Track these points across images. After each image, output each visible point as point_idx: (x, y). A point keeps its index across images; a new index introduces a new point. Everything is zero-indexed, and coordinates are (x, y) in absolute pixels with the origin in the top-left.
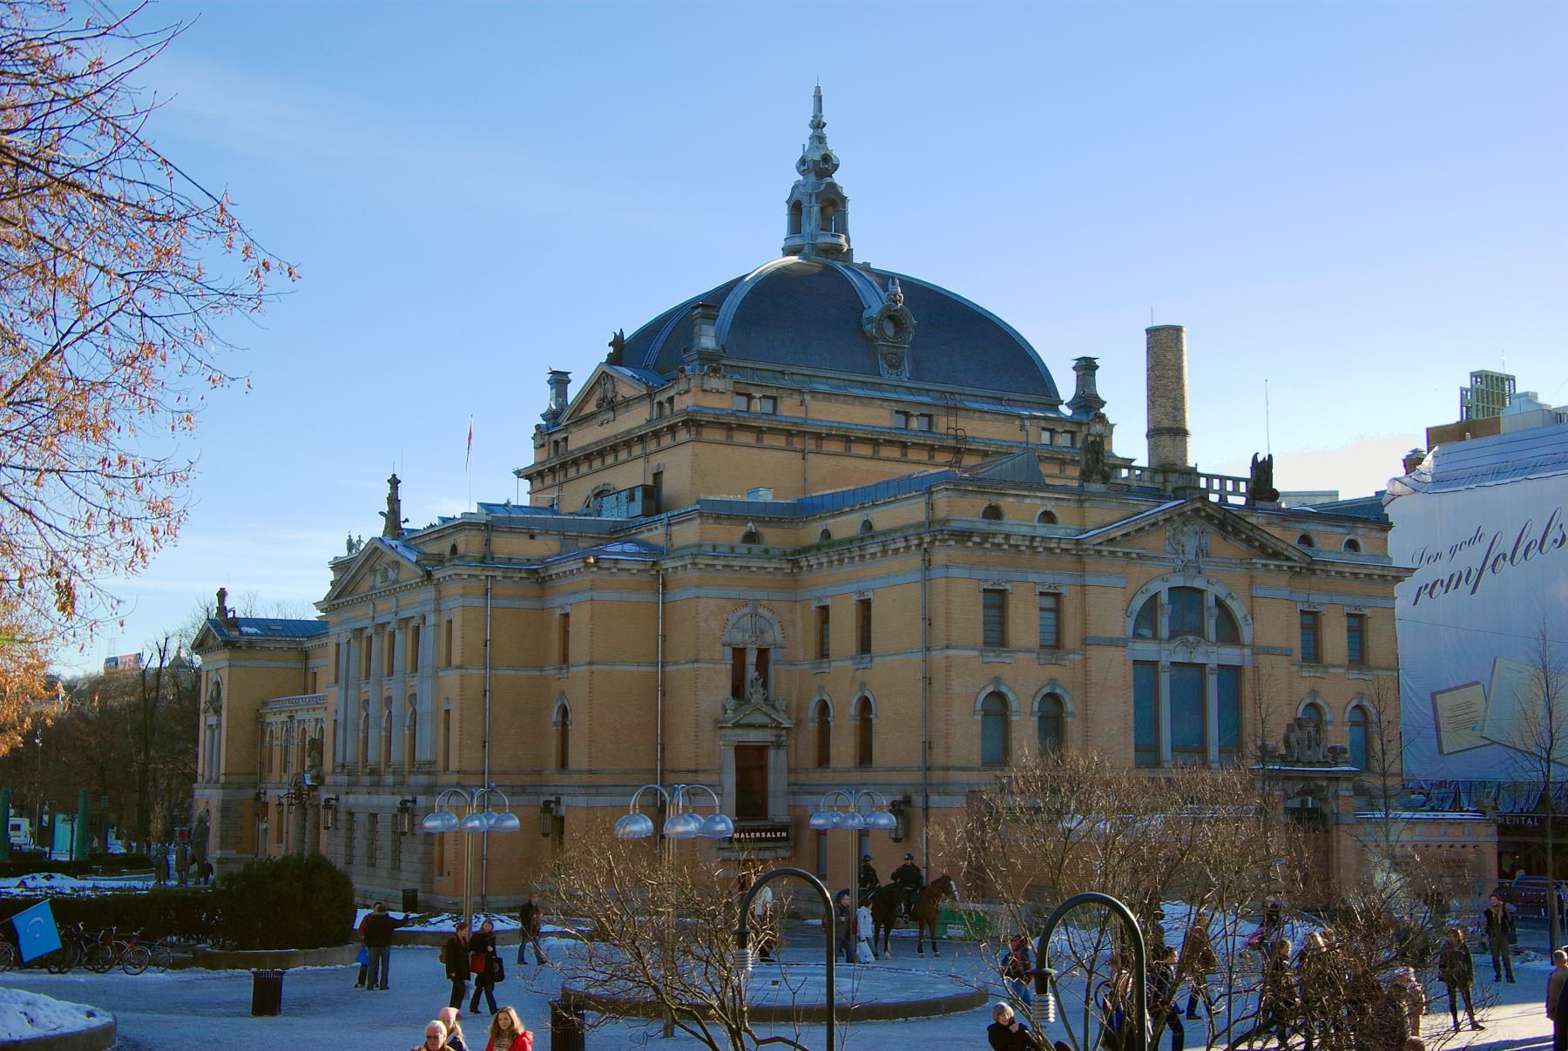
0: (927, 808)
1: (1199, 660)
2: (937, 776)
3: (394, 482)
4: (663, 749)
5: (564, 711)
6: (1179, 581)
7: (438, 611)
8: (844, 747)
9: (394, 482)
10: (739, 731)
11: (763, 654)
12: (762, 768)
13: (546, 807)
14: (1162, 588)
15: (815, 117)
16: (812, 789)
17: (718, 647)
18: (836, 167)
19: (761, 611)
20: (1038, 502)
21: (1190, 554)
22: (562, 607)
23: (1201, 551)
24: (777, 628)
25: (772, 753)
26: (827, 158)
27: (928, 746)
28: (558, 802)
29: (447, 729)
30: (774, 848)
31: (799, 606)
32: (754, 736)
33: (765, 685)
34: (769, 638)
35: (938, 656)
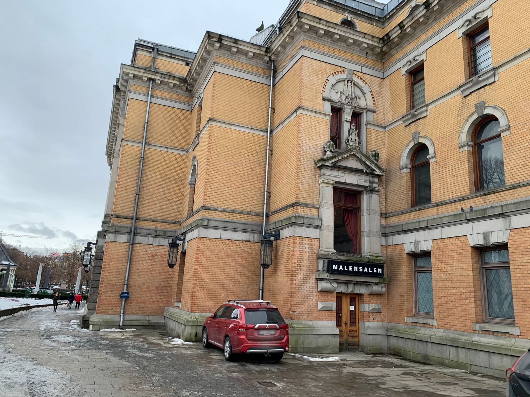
4: (269, 196)
8: (450, 177)
10: (336, 173)
11: (356, 116)
19: (355, 79)
30: (367, 284)
31: (387, 81)
33: (359, 136)
34: (362, 103)
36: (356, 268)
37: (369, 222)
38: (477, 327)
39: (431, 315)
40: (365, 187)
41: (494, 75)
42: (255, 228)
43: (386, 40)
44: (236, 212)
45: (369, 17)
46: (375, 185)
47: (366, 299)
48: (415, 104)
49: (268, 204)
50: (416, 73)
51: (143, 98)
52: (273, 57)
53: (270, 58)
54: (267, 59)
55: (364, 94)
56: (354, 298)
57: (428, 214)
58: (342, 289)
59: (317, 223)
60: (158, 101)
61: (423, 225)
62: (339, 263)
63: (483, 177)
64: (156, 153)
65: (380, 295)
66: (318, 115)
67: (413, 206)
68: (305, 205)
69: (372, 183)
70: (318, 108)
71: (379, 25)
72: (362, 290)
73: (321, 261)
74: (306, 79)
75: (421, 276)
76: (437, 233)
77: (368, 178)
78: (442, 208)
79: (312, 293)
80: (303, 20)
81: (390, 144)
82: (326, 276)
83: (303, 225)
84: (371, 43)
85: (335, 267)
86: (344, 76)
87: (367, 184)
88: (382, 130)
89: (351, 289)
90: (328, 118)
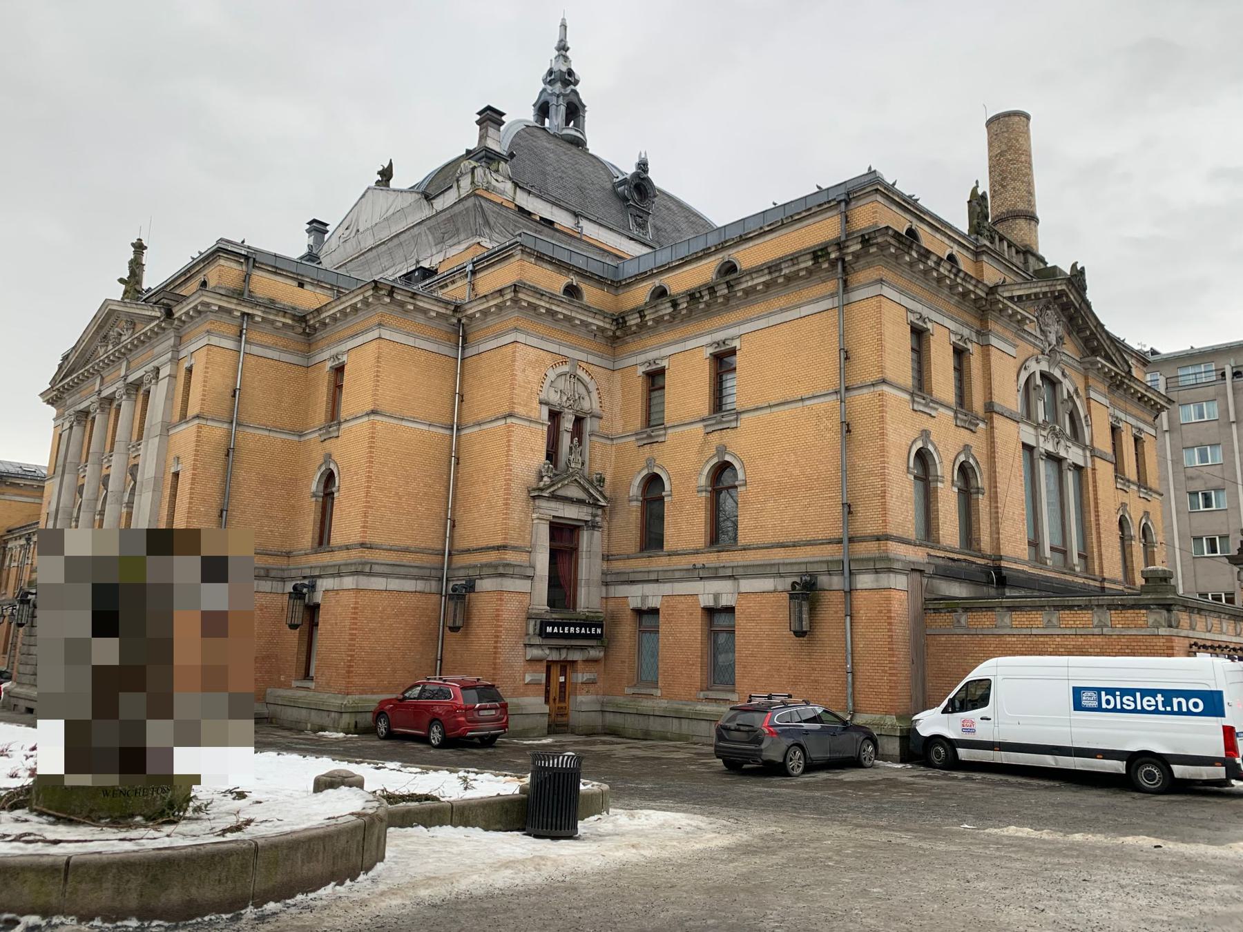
0: (850, 592)
1: (1063, 454)
2: (865, 549)
3: (139, 247)
4: (453, 526)
5: (329, 478)
6: (1044, 366)
7: (176, 360)
8: (685, 523)
9: (139, 247)
10: (553, 505)
11: (579, 421)
12: (573, 551)
13: (297, 593)
14: (1035, 367)
15: (561, 41)
16: (632, 577)
17: (535, 404)
18: (576, 82)
19: (581, 373)
20: (947, 241)
21: (1053, 338)
22: (336, 357)
23: (1060, 340)
24: (595, 395)
25: (585, 536)
26: (570, 73)
27: (849, 509)
28: (312, 587)
29: (174, 496)
30: (582, 648)
31: (617, 375)
32: (570, 512)
34: (586, 405)
35: (862, 398)
36: (572, 629)
37: (589, 567)
38: (702, 695)
39: (655, 685)
40: (586, 522)
41: (737, 420)
42: (434, 573)
43: (620, 320)
44: (406, 550)
45: (600, 281)
46: (598, 519)
47: (580, 666)
48: (652, 421)
49: (452, 537)
50: (655, 378)
51: (230, 344)
52: (464, 321)
53: (459, 320)
54: (455, 321)
55: (589, 392)
56: (566, 666)
57: (659, 563)
58: (554, 656)
59: (529, 572)
60: (256, 350)
61: (653, 577)
62: (553, 625)
63: (720, 531)
64: (251, 438)
65: (596, 661)
66: (533, 425)
67: (642, 550)
68: (514, 548)
69: (594, 516)
70: (534, 415)
71: (612, 290)
72: (576, 656)
73: (532, 623)
74: (520, 377)
75: (646, 637)
76: (666, 589)
77: (590, 510)
78: (675, 559)
79: (519, 663)
80: (521, 295)
81: (615, 460)
82: (538, 641)
83: (512, 576)
84: (601, 324)
85: (549, 629)
86: (566, 368)
87: (589, 518)
88: (609, 442)
89: (564, 655)
90: (546, 428)
